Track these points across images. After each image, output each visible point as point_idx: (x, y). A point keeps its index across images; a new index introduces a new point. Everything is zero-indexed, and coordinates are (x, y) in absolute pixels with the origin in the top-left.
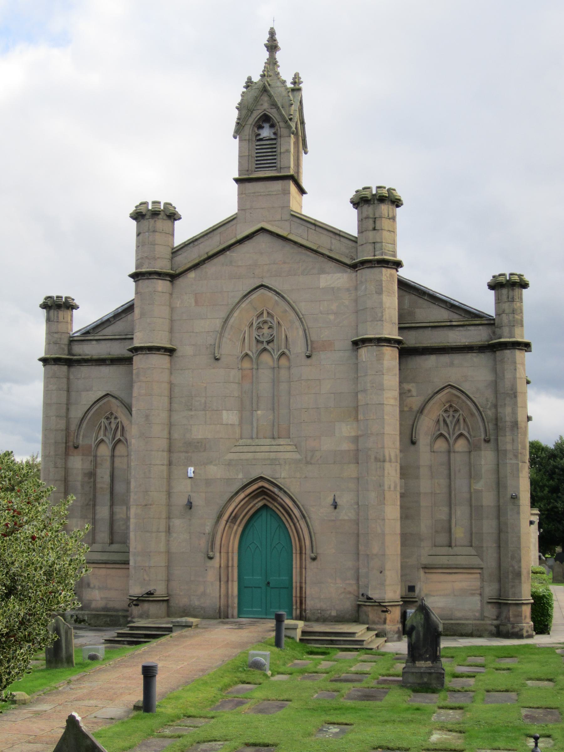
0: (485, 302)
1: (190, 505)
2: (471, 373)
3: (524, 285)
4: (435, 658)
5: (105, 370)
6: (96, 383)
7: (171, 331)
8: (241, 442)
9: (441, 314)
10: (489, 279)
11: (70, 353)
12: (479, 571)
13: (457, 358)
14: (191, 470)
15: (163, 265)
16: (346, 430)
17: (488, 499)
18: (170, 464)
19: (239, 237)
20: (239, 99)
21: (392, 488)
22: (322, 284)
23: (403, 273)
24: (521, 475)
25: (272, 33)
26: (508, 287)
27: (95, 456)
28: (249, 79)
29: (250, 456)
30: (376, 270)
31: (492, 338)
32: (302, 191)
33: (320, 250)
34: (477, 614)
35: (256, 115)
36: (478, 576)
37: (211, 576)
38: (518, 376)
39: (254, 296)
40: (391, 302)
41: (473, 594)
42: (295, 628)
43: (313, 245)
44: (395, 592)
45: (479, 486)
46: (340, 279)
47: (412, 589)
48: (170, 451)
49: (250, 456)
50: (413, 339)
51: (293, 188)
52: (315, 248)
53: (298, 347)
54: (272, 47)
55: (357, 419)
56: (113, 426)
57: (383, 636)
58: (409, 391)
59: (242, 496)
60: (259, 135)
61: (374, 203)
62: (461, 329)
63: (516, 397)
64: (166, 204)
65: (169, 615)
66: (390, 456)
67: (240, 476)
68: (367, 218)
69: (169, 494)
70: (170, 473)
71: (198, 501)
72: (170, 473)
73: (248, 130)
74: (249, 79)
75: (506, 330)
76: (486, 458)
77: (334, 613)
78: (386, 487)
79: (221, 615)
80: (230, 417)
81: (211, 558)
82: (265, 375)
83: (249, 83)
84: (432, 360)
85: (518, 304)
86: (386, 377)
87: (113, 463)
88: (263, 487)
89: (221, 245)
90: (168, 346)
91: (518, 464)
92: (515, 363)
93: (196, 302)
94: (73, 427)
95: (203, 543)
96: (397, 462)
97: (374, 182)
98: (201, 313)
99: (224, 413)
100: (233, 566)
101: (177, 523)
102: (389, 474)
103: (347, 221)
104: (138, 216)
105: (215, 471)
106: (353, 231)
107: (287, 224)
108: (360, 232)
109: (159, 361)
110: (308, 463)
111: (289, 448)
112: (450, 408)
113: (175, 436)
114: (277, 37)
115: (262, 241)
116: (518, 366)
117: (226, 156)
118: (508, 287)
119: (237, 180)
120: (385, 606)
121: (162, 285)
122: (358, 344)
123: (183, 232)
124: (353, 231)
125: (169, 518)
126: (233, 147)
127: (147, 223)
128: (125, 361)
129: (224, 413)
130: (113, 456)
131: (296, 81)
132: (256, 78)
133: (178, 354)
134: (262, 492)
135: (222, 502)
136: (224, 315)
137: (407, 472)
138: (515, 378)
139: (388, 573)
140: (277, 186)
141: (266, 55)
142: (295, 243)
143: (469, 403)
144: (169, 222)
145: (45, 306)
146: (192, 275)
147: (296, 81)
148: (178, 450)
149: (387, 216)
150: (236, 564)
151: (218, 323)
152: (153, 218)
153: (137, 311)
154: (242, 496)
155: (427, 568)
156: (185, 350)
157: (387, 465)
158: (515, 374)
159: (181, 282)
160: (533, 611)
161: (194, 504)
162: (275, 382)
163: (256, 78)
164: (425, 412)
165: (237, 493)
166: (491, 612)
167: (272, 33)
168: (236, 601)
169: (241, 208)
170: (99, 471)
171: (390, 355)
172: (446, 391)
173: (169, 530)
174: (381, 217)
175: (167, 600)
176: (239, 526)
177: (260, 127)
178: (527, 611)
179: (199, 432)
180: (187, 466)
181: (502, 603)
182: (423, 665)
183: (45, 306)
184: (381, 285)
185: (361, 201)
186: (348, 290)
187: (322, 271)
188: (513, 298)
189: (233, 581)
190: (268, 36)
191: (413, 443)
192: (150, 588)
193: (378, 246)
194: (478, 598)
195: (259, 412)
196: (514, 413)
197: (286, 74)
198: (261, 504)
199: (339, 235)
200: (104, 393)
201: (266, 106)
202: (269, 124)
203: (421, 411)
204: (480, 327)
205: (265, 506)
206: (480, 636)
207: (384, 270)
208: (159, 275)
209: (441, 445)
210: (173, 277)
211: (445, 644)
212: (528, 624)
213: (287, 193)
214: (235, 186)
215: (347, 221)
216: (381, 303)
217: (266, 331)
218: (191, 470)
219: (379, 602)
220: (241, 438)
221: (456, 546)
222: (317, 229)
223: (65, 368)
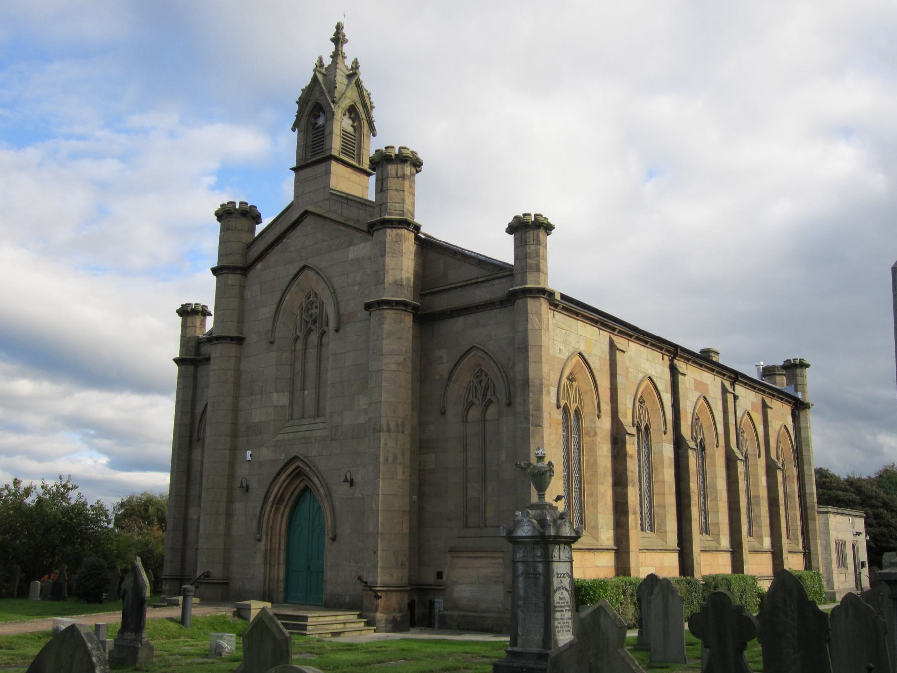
7: (241, 320)
8: (290, 423)
9: (472, 272)
11: (198, 353)
12: (501, 555)
13: (482, 316)
14: (249, 452)
20: (300, 93)
21: (390, 459)
22: (351, 257)
24: (532, 440)
25: (339, 27)
26: (528, 230)
29: (291, 436)
30: (381, 232)
33: (347, 223)
34: (500, 606)
36: (501, 561)
37: (259, 559)
38: (530, 326)
39: (301, 278)
40: (403, 264)
42: (248, 608)
44: (391, 576)
47: (439, 575)
49: (291, 436)
52: (343, 221)
53: (332, 324)
54: (338, 39)
57: (373, 625)
58: (441, 358)
59: (284, 476)
60: (316, 124)
62: (487, 284)
63: (527, 351)
64: (241, 203)
66: (388, 425)
67: (283, 457)
69: (231, 477)
71: (253, 485)
73: (304, 121)
75: (518, 278)
77: (348, 599)
78: (381, 459)
80: (282, 399)
82: (312, 353)
84: (460, 322)
85: (533, 247)
86: (385, 342)
88: (298, 467)
90: (233, 333)
91: (529, 428)
92: (527, 312)
96: (397, 431)
100: (279, 549)
101: (238, 506)
102: (386, 444)
105: (266, 453)
107: (327, 202)
109: (231, 350)
110: (333, 439)
111: (322, 426)
112: (480, 373)
113: (241, 421)
114: (345, 31)
115: (309, 224)
116: (530, 316)
120: (375, 592)
121: (232, 279)
129: (275, 395)
133: (246, 342)
134: (299, 473)
135: (268, 484)
136: (278, 299)
138: (526, 330)
139: (379, 553)
140: (321, 168)
141: (332, 47)
142: (332, 220)
143: (492, 364)
146: (259, 266)
149: (394, 174)
150: (282, 547)
151: (274, 307)
154: (284, 476)
156: (252, 338)
157: (384, 436)
158: (527, 324)
159: (252, 274)
161: (251, 486)
162: (320, 359)
164: (454, 378)
165: (279, 474)
167: (339, 27)
168: (281, 586)
169: (296, 196)
172: (472, 354)
173: (229, 515)
174: (387, 177)
175: (227, 584)
176: (285, 507)
177: (317, 117)
179: (258, 415)
180: (247, 450)
182: (129, 635)
184: (385, 245)
186: (370, 258)
187: (351, 244)
188: (526, 241)
189: (278, 564)
190: (335, 30)
191: (443, 413)
192: (206, 570)
193: (384, 206)
195: (306, 392)
196: (526, 370)
198: (302, 485)
199: (366, 205)
201: (318, 94)
203: (450, 378)
204: (504, 280)
207: (388, 231)
210: (244, 270)
213: (328, 173)
214: (293, 174)
216: (384, 265)
217: (314, 311)
218: (249, 452)
219: (370, 587)
220: (291, 419)
221: (486, 527)
222: (350, 203)
223: (191, 368)
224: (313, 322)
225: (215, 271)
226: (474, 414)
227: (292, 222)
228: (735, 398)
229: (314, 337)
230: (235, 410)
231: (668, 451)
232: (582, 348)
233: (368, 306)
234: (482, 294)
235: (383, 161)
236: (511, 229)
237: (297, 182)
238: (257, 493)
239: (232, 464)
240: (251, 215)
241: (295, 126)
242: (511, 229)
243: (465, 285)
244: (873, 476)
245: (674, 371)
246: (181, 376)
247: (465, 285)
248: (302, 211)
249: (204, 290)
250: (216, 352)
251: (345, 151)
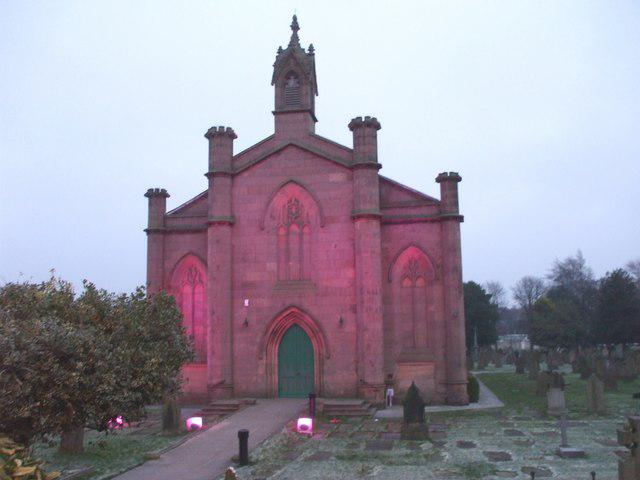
0: (434, 191)
1: (246, 323)
2: (428, 235)
3: (459, 179)
4: (422, 420)
5: (188, 237)
6: (183, 244)
9: (406, 198)
10: (436, 176)
13: (417, 226)
14: (246, 302)
15: (226, 168)
16: (349, 273)
17: (438, 317)
18: (232, 298)
19: (276, 149)
22: (331, 180)
23: (381, 172)
25: (295, 18)
26: (449, 181)
27: (182, 294)
28: (280, 47)
31: (441, 213)
32: (315, 120)
41: (429, 378)
43: (326, 153)
45: (432, 308)
46: (338, 177)
47: (390, 376)
48: (232, 288)
50: (388, 213)
51: (310, 118)
54: (295, 27)
55: (354, 266)
56: (194, 273)
61: (365, 129)
65: (233, 396)
68: (359, 137)
70: (232, 303)
72: (232, 303)
74: (280, 47)
76: (437, 291)
79: (267, 395)
80: (272, 266)
81: (261, 359)
83: (280, 50)
84: (401, 228)
87: (193, 298)
89: (263, 153)
93: (248, 191)
94: (168, 274)
97: (363, 113)
98: (249, 198)
99: (268, 264)
101: (238, 336)
103: (346, 139)
105: (265, 302)
106: (350, 145)
108: (356, 144)
109: (225, 229)
115: (291, 151)
117: (268, 96)
118: (449, 181)
119: (274, 113)
122: (355, 218)
123: (239, 147)
124: (350, 145)
125: (232, 333)
127: (217, 140)
128: (202, 231)
130: (193, 293)
131: (311, 48)
132: (285, 47)
137: (387, 300)
140: (301, 116)
141: (291, 32)
144: (229, 139)
145: (146, 195)
146: (246, 174)
147: (311, 48)
148: (237, 288)
152: (220, 138)
153: (209, 198)
155: (401, 361)
159: (240, 180)
160: (468, 388)
162: (301, 242)
163: (285, 47)
166: (442, 389)
167: (295, 18)
170: (184, 303)
171: (375, 226)
178: (465, 387)
179: (252, 276)
181: (448, 383)
183: (146, 195)
185: (356, 125)
191: (390, 281)
194: (432, 380)
197: (304, 45)
200: (187, 252)
202: (295, 73)
205: (296, 324)
206: (435, 405)
208: (224, 174)
209: (407, 282)
211: (427, 409)
212: (465, 396)
213: (305, 120)
215: (346, 139)
218: (246, 302)
224: (294, 217)
230: (232, 271)
234: (414, 213)
237: (277, 122)
240: (230, 135)
241: (275, 81)
243: (402, 206)
247: (402, 206)
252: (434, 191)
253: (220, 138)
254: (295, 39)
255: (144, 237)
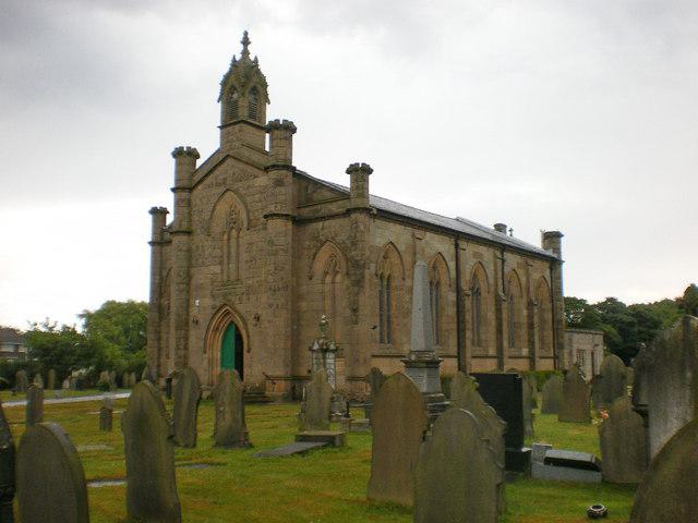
0: (345, 181)
9: (328, 195)
25: (246, 34)
35: (228, 86)
50: (306, 212)
54: (246, 42)
95: (202, 344)
104: (178, 153)
109: (184, 238)
115: (229, 161)
126: (219, 107)
131: (256, 58)
141: (241, 47)
147: (256, 58)
152: (185, 156)
159: (195, 192)
167: (246, 34)
210: (191, 189)
223: (158, 247)
225: (173, 190)
226: (328, 279)
227: (217, 161)
228: (503, 261)
229: (234, 232)
231: (452, 297)
232: (393, 239)
233: (266, 217)
234: (334, 208)
235: (275, 127)
236: (348, 172)
238: (203, 324)
239: (188, 306)
240: (193, 154)
242: (348, 172)
244: (627, 305)
245: (457, 246)
246: (153, 253)
248: (225, 154)
249: (168, 201)
250: (176, 239)
251: (252, 116)
252: (345, 181)
253: (185, 156)
254: (245, 53)
255: (149, 249)
